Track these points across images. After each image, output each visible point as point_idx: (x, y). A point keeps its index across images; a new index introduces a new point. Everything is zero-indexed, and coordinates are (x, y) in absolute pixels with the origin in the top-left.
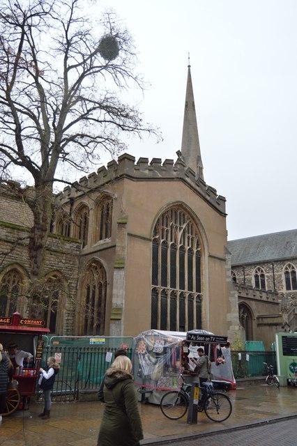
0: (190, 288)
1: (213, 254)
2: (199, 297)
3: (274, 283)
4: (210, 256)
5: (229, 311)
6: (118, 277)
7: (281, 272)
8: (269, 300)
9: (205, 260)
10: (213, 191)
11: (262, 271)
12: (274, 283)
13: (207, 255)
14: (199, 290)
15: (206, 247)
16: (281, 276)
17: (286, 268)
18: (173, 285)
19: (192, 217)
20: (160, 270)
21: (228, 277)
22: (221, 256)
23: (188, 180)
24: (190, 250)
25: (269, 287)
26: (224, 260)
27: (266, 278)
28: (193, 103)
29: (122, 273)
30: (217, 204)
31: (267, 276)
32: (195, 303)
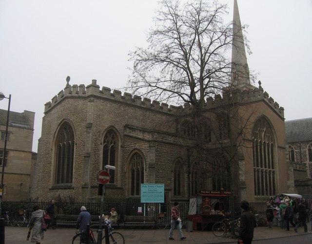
0: (269, 168)
1: (280, 145)
2: (274, 172)
3: (301, 156)
4: (278, 147)
5: (288, 179)
6: (242, 164)
7: (306, 149)
8: (301, 169)
9: (276, 149)
10: (277, 105)
11: (292, 148)
12: (301, 156)
13: (276, 146)
14: (273, 168)
15: (276, 141)
16: (305, 152)
17: (309, 147)
18: (262, 167)
19: (268, 123)
20: (255, 158)
21: (287, 159)
22: (283, 146)
23: (266, 100)
24: (268, 144)
25: (297, 159)
26: (285, 148)
27: (295, 153)
28: (240, 21)
29: (244, 162)
30: (279, 112)
31: (296, 152)
32: (272, 176)
